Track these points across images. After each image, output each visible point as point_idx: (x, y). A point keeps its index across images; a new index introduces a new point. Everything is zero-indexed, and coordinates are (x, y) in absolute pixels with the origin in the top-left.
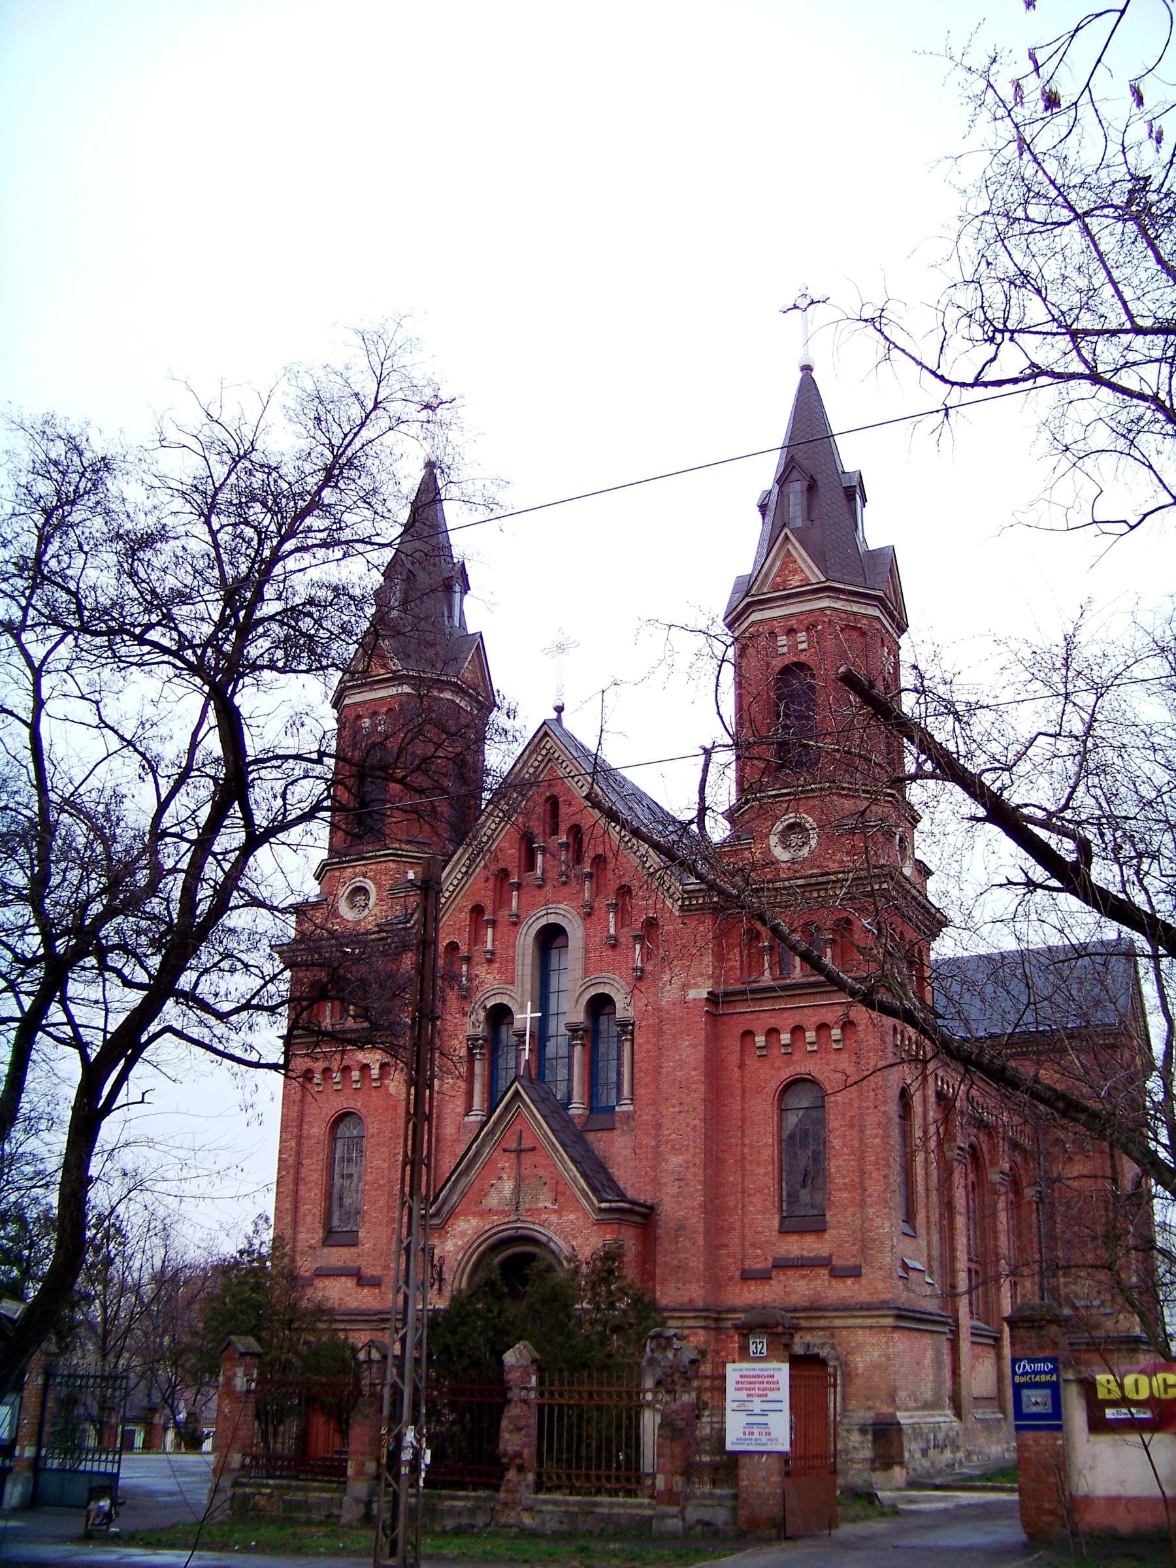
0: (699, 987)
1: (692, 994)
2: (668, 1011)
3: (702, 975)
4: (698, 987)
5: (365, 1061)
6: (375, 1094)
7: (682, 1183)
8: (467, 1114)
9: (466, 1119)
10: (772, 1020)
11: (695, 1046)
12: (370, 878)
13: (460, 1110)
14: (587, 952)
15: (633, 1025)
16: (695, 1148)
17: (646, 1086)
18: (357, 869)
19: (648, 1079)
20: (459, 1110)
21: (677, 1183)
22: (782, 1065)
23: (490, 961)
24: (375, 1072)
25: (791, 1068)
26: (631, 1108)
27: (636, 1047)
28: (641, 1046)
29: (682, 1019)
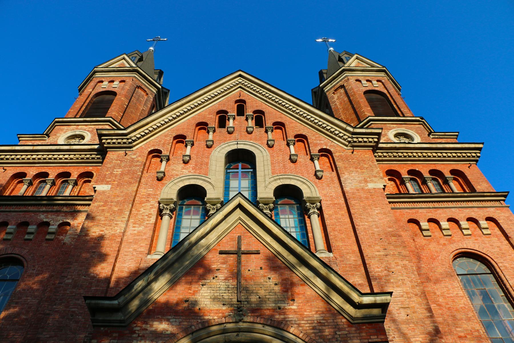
0: (375, 182)
1: (371, 186)
2: (353, 193)
3: (375, 177)
4: (372, 181)
5: (45, 220)
6: (44, 244)
7: (409, 312)
8: (149, 253)
9: (149, 257)
10: (430, 214)
11: (385, 214)
12: (88, 131)
13: (145, 250)
14: (272, 164)
15: (320, 202)
16: (411, 282)
17: (343, 240)
18: (80, 127)
19: (343, 236)
20: (142, 249)
21: (402, 310)
22: (446, 242)
23: (185, 162)
24: (53, 228)
25: (455, 244)
26: (331, 255)
27: (326, 216)
28: (330, 216)
29: (367, 198)
